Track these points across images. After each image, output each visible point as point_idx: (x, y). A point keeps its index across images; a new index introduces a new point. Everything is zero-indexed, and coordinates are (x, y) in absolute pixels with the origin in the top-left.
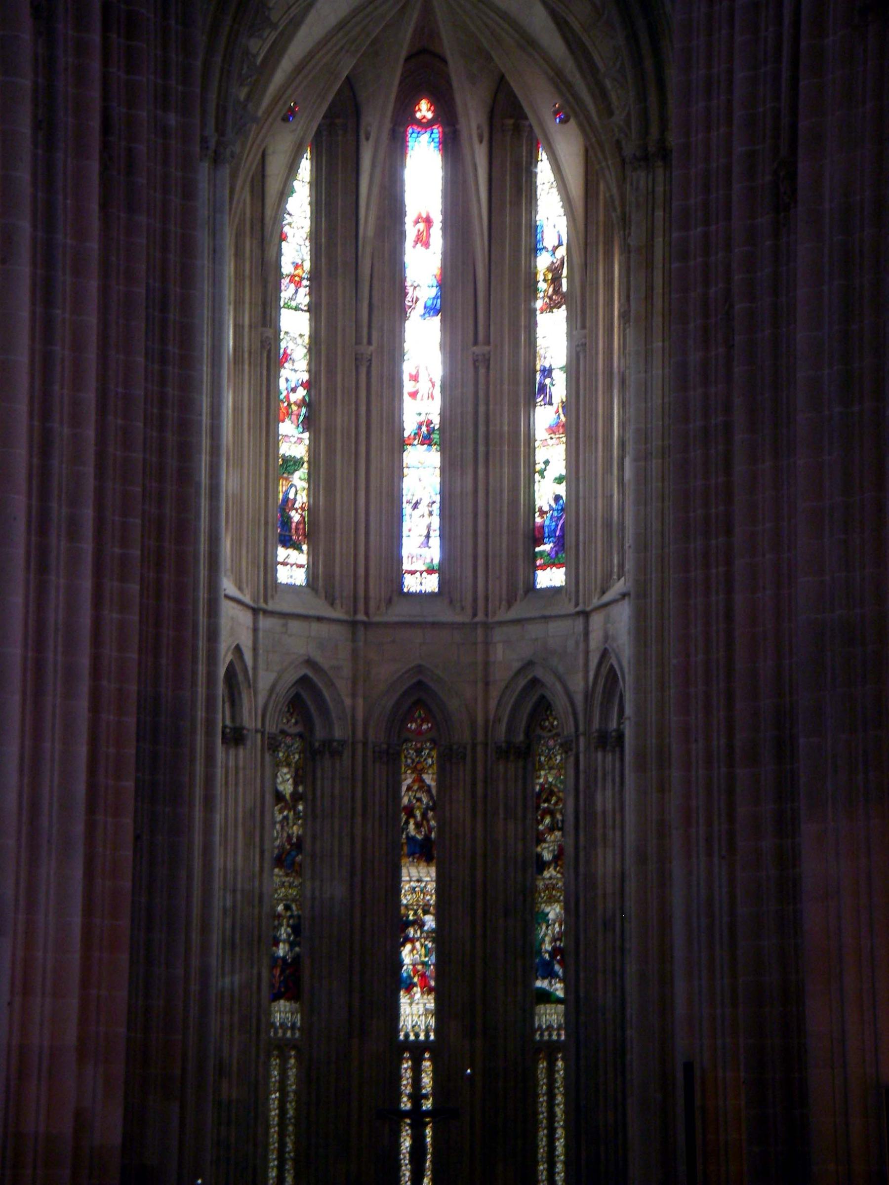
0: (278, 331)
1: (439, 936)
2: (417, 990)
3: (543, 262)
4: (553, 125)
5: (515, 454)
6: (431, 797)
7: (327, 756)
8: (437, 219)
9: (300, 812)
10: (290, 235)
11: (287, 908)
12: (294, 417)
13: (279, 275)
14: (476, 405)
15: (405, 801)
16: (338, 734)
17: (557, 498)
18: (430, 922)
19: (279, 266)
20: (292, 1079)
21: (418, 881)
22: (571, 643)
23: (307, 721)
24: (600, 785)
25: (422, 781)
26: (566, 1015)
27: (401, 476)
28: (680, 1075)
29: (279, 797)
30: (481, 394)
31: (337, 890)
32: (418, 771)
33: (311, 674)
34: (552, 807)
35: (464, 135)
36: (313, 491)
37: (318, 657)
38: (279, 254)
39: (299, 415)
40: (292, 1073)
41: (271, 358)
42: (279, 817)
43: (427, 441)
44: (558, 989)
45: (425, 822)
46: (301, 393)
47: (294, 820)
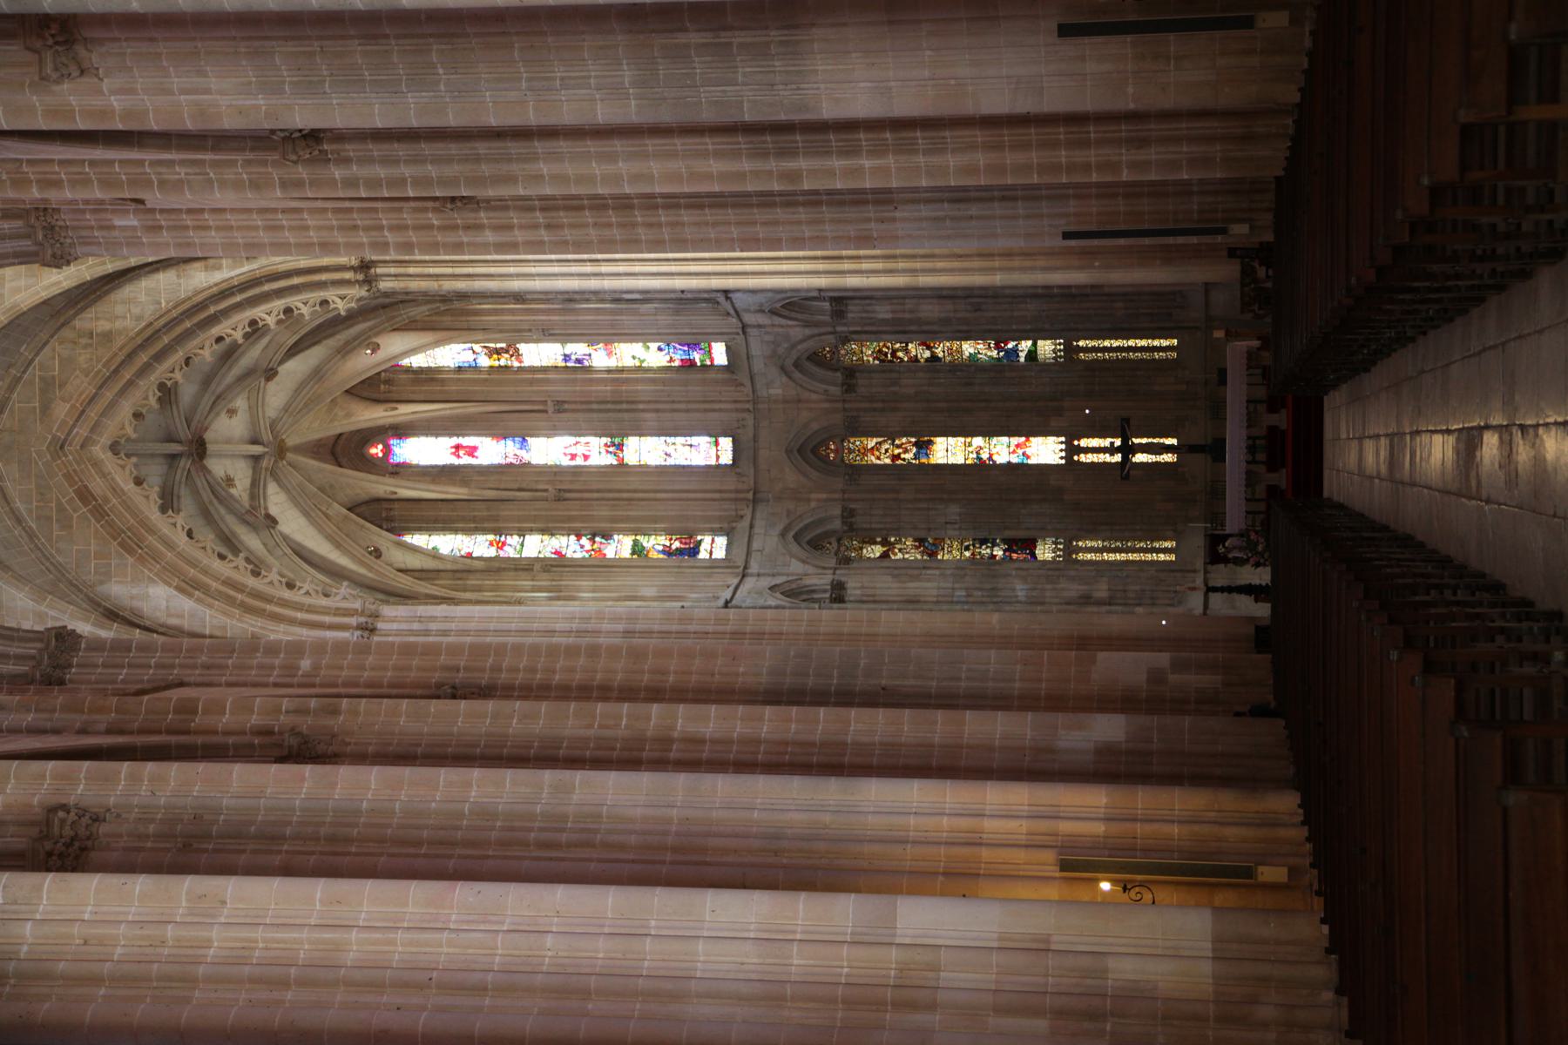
0: (537, 559)
1: (989, 432)
2: (1028, 451)
3: (484, 362)
4: (381, 355)
5: (627, 381)
8: (455, 441)
11: (967, 548)
13: (497, 558)
14: (608, 411)
15: (888, 461)
16: (837, 511)
17: (660, 349)
18: (978, 441)
19: (490, 559)
20: (1094, 544)
22: (767, 338)
23: (827, 535)
26: (1044, 339)
27: (647, 466)
28: (1073, 243)
29: (885, 555)
31: (954, 511)
32: (866, 451)
35: (390, 421)
36: (656, 532)
37: (781, 527)
38: (480, 559)
40: (1089, 544)
41: (557, 565)
42: (900, 556)
43: (620, 447)
44: (1026, 345)
46: (584, 541)
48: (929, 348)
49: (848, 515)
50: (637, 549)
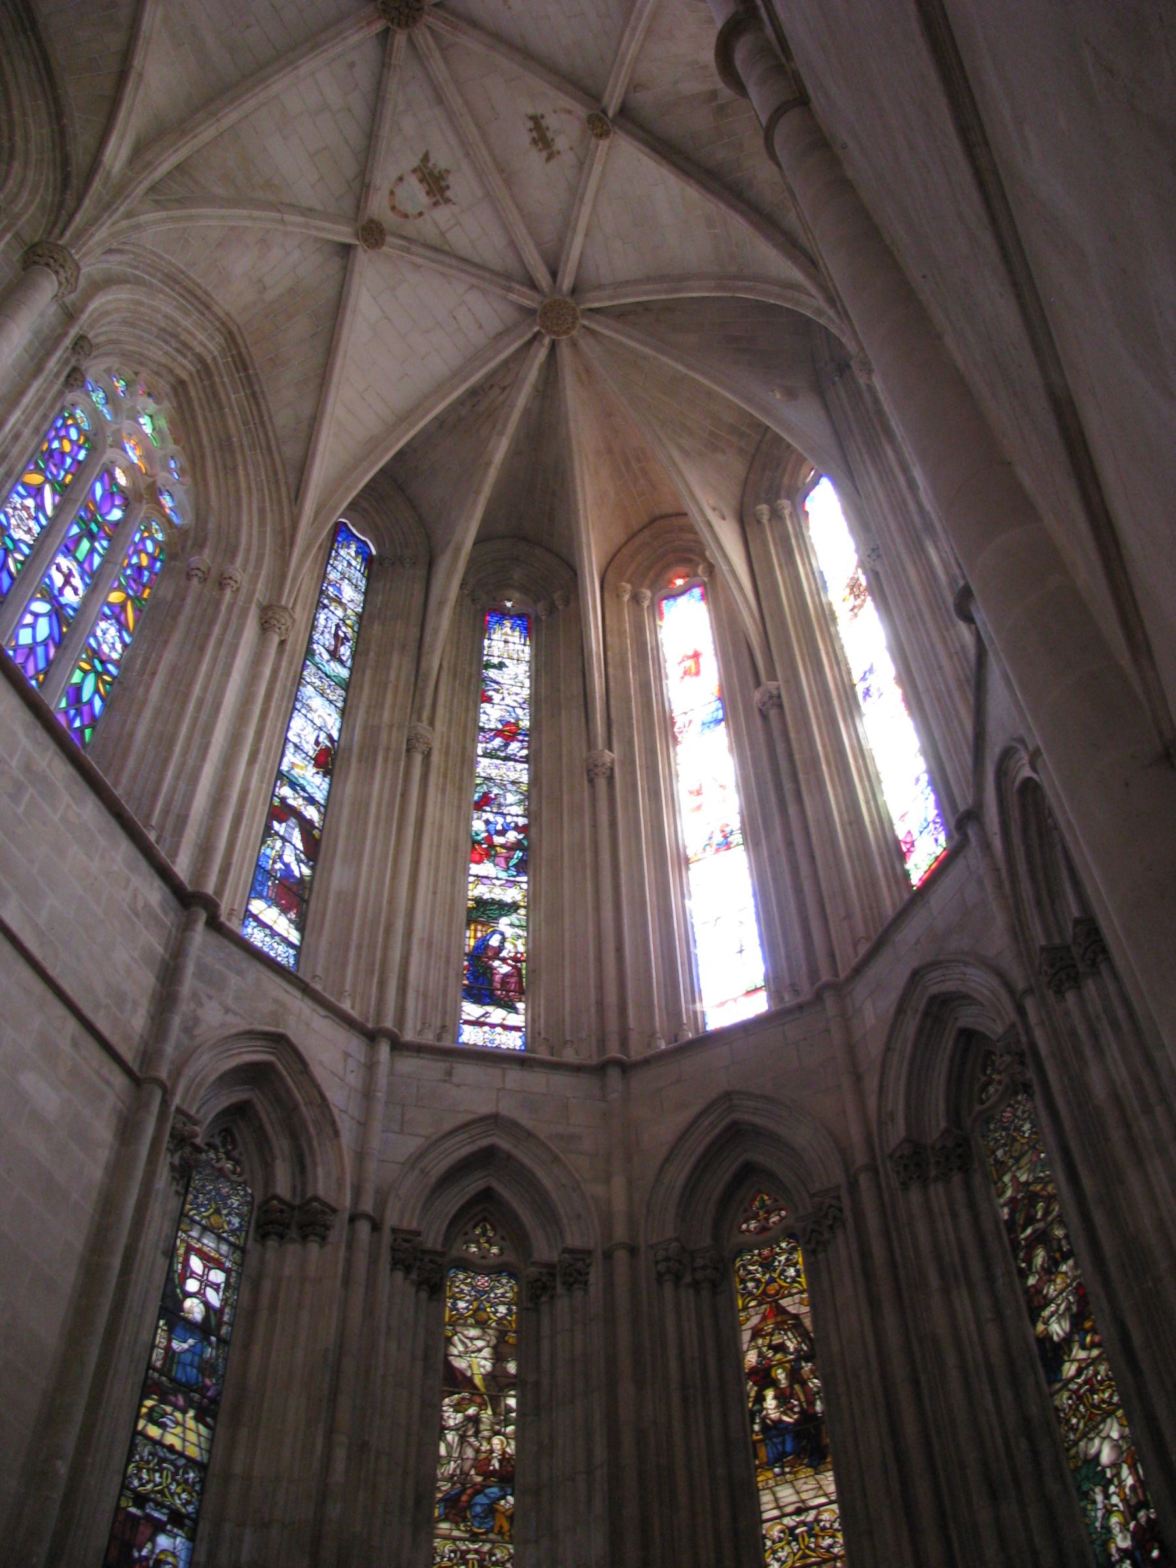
6: (803, 1334)
7: (560, 1289)
9: (509, 1410)
10: (497, 698)
12: (502, 861)
15: (751, 1358)
16: (574, 1239)
21: (798, 1512)
24: (1088, 1052)
25: (783, 1311)
29: (456, 1380)
30: (777, 734)
33: (504, 1144)
34: (1041, 1225)
39: (508, 859)
45: (797, 1387)
47: (493, 1424)
48: (1077, 1321)
49: (572, 1271)
50: (487, 911)
